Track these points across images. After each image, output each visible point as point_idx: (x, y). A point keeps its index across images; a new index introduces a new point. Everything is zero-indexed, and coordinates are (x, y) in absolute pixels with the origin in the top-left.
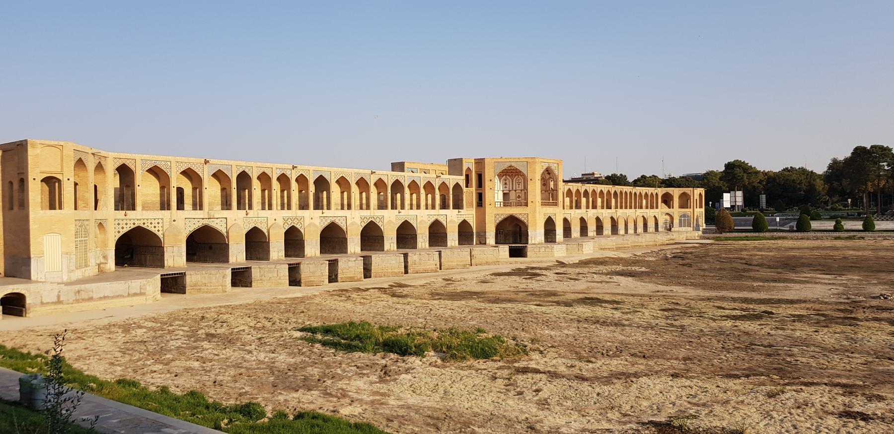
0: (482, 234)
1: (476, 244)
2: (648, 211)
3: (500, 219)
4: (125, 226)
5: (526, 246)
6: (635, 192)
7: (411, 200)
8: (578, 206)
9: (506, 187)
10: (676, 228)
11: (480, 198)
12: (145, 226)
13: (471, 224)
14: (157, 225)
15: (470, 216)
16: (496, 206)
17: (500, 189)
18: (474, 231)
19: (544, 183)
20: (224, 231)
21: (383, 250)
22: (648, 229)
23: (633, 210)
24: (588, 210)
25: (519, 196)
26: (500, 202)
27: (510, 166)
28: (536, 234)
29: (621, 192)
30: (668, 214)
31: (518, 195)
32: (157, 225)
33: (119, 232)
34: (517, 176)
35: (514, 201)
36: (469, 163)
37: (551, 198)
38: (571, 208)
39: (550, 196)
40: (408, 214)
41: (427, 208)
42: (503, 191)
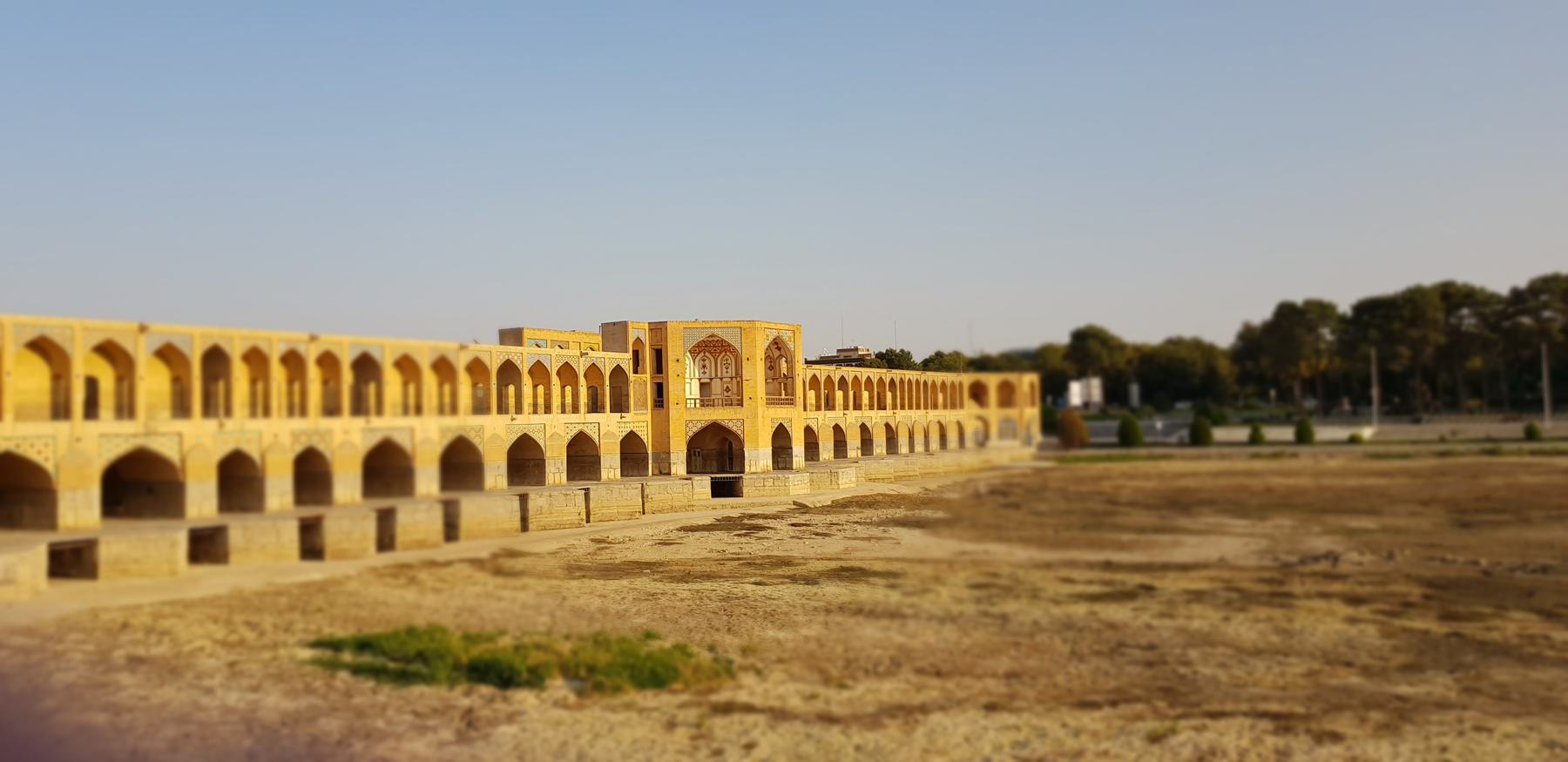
1: (653, 475)
3: (695, 430)
6: (925, 381)
7: (535, 396)
8: (830, 406)
9: (704, 373)
10: (994, 441)
11: (660, 390)
13: (644, 438)
15: (642, 424)
16: (688, 406)
17: (694, 375)
18: (650, 452)
19: (771, 364)
23: (922, 412)
24: (845, 412)
25: (727, 387)
26: (695, 399)
27: (712, 336)
28: (758, 456)
29: (902, 381)
30: (980, 418)
31: (725, 386)
34: (724, 353)
35: (718, 397)
37: (783, 392)
38: (818, 408)
39: (781, 387)
40: (529, 423)
41: (563, 411)
42: (700, 379)
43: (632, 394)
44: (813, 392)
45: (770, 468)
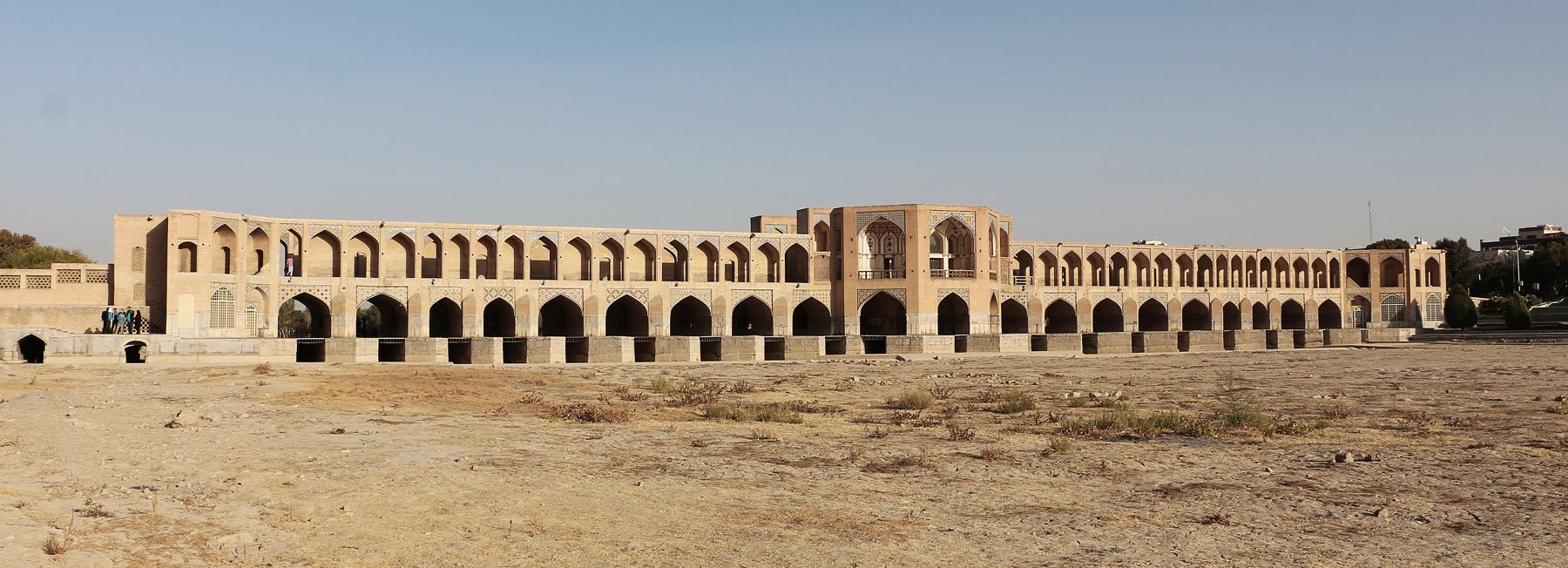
4: (289, 292)
12: (311, 293)
14: (324, 292)
15: (822, 292)
20: (404, 302)
22: (1306, 323)
32: (324, 292)
33: (283, 298)
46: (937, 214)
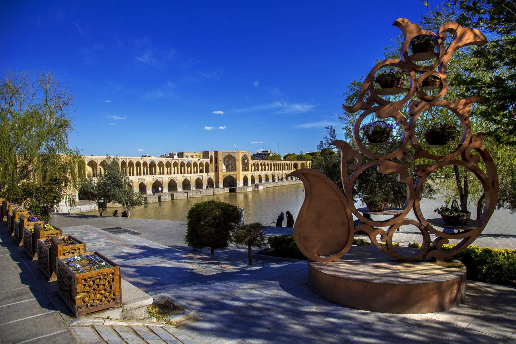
0: (217, 183)
2: (288, 171)
3: (225, 177)
5: (236, 188)
8: (258, 170)
13: (213, 179)
18: (214, 182)
19: (243, 161)
21: (177, 191)
27: (229, 154)
28: (240, 184)
36: (211, 153)
37: (246, 167)
39: (245, 166)
40: (187, 176)
41: (194, 173)
43: (210, 168)
44: (254, 167)
45: (243, 186)
46: (242, 153)
